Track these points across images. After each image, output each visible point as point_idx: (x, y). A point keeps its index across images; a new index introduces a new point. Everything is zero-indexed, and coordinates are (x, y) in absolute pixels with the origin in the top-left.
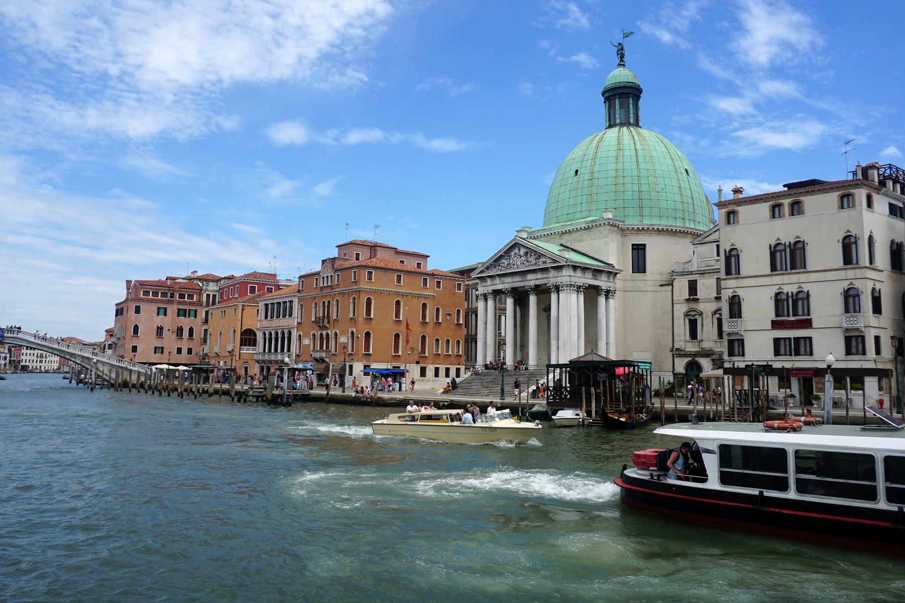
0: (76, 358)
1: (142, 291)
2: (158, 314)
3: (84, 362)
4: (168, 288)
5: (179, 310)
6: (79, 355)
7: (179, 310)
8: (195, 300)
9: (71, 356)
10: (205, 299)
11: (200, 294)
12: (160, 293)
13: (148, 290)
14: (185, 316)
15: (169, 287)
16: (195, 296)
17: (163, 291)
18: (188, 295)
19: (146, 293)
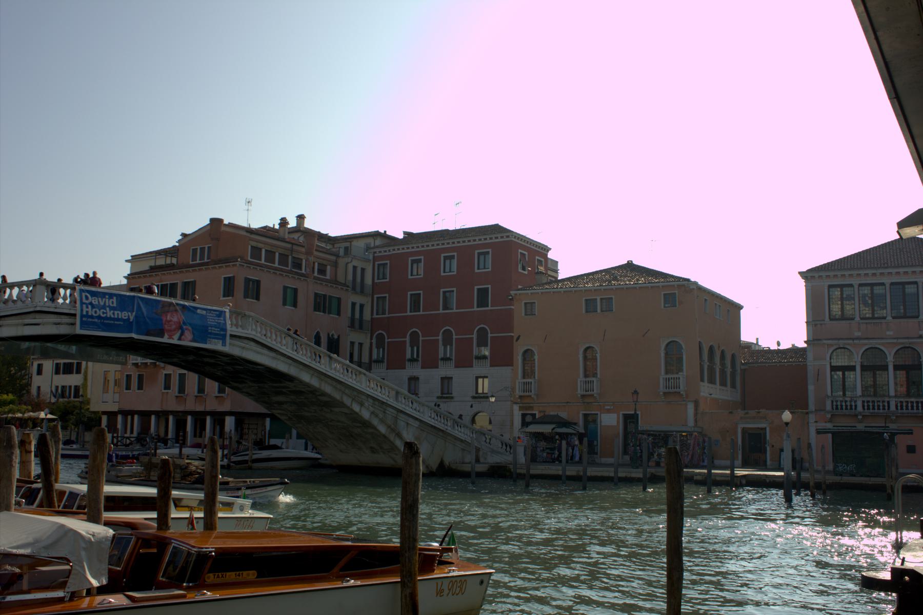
0: (362, 405)
1: (250, 247)
2: (284, 304)
3: (377, 416)
4: (289, 246)
5: (316, 294)
6: (368, 396)
7: (316, 294)
8: (328, 277)
9: (353, 399)
10: (350, 277)
11: (335, 265)
12: (277, 255)
13: (260, 245)
14: (324, 312)
15: (293, 244)
16: (329, 267)
17: (282, 251)
18: (319, 264)
19: (256, 251)
